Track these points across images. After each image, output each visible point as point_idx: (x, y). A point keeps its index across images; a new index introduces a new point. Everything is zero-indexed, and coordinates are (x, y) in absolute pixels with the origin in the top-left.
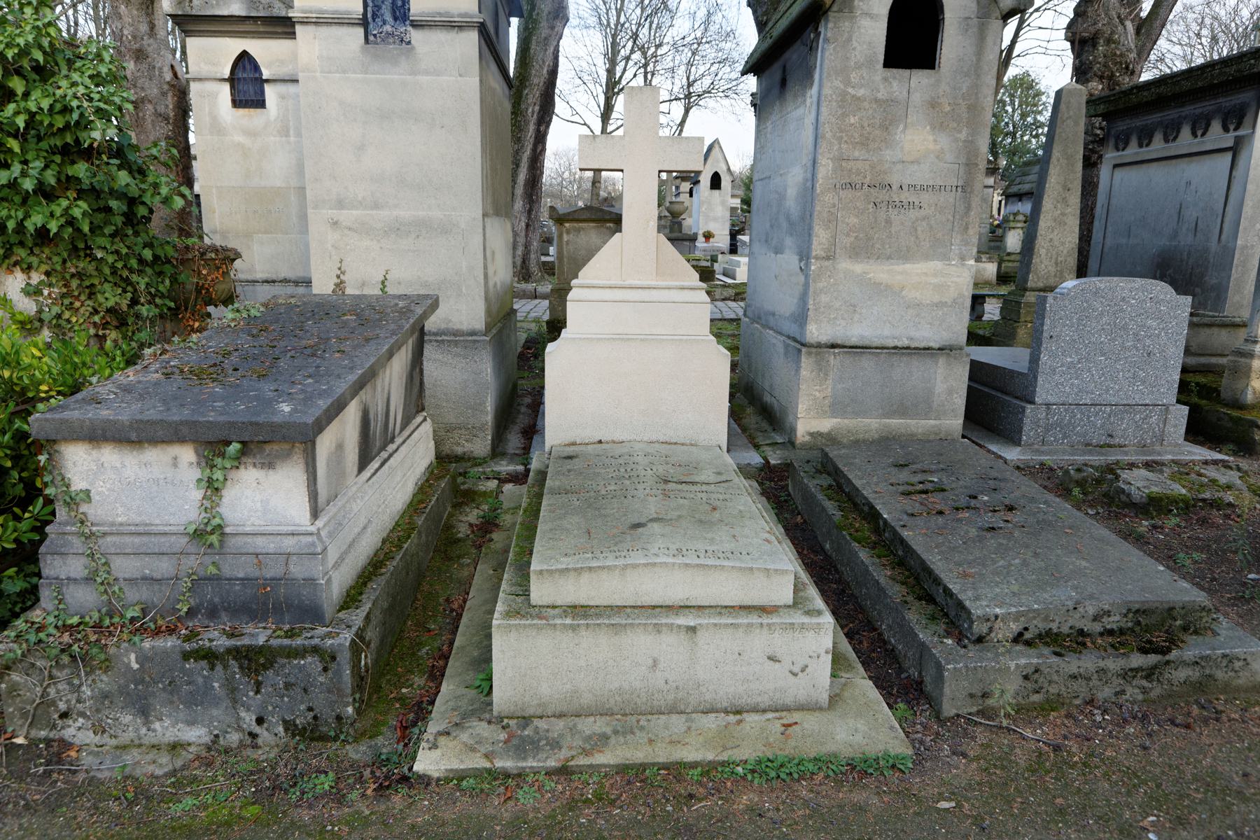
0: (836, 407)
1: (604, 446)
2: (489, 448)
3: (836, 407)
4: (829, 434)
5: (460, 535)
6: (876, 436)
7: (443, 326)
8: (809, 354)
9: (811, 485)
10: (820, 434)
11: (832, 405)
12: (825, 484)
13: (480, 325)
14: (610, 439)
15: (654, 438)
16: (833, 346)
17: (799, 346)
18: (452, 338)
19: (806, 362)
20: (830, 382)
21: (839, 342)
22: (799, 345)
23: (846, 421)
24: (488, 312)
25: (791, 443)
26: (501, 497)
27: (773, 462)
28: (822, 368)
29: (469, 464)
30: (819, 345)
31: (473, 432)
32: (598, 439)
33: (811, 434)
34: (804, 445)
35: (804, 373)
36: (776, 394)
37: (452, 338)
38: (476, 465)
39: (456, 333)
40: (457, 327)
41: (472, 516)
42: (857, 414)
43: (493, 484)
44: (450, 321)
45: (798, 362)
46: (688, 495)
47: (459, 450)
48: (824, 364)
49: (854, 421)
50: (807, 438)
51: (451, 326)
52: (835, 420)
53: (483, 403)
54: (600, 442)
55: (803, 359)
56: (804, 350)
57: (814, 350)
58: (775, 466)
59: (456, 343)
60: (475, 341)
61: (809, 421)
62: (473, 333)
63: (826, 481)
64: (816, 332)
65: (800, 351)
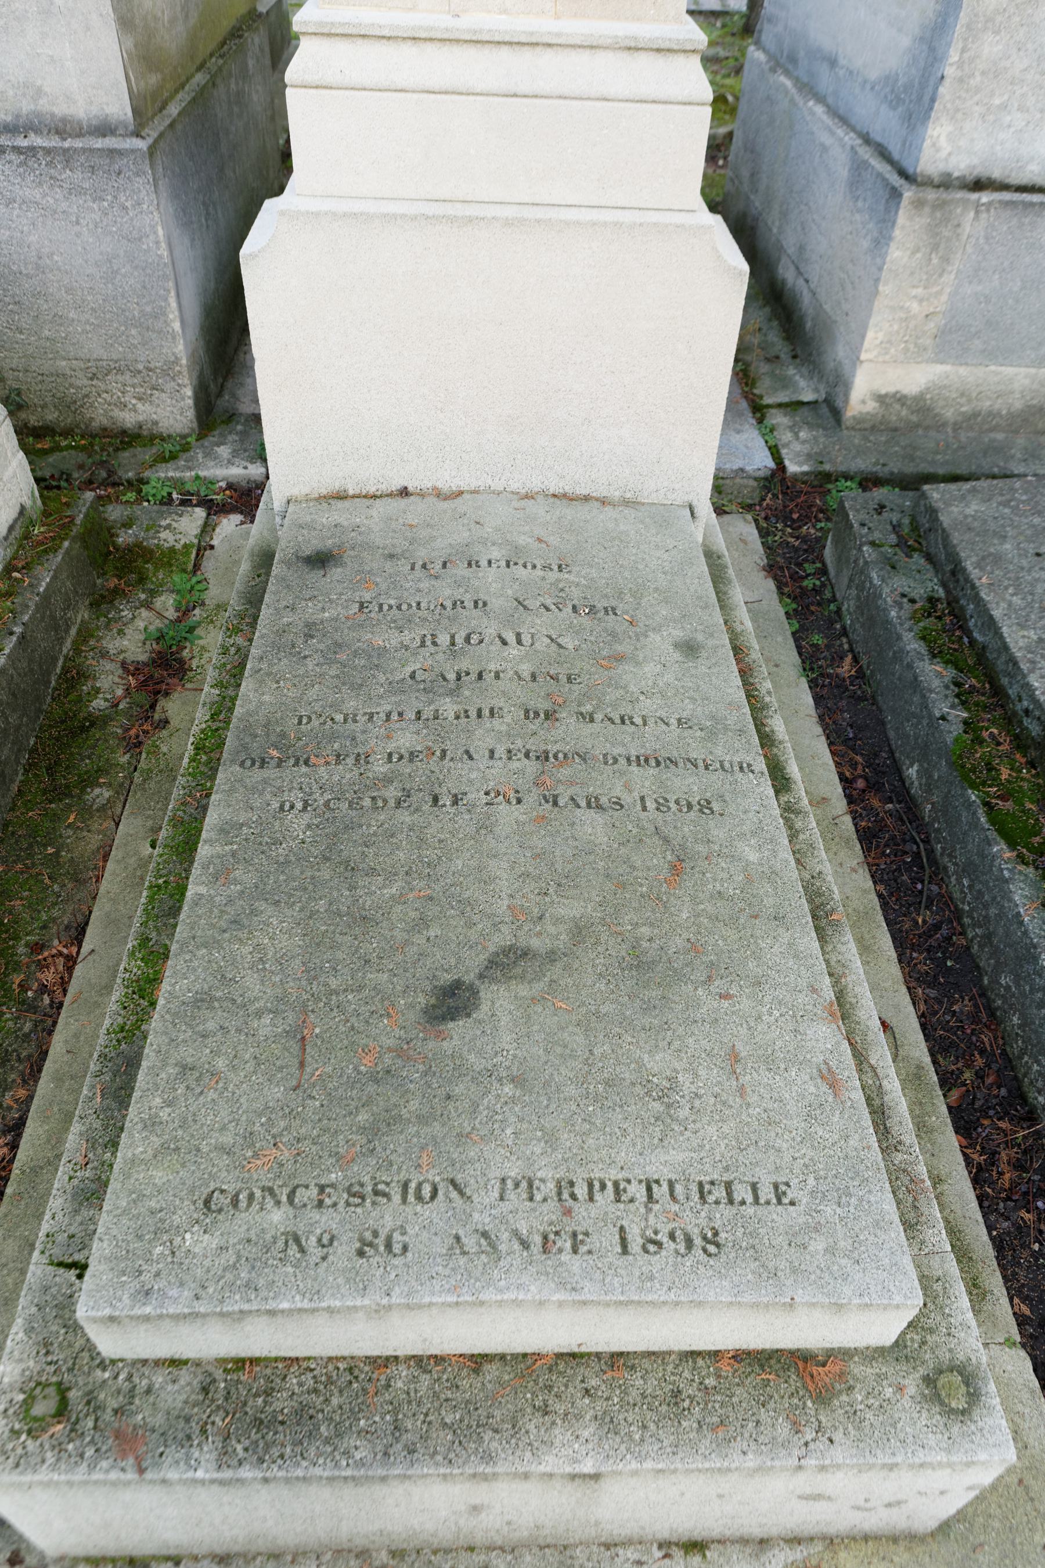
0: (951, 339)
1: (414, 511)
2: (191, 414)
3: (951, 339)
4: (919, 398)
5: (99, 704)
6: (1018, 405)
7: (26, 107)
8: (919, 204)
9: (888, 595)
10: (900, 399)
11: (943, 335)
12: (919, 592)
13: (118, 106)
14: (427, 485)
15: (535, 483)
16: (979, 185)
17: (895, 180)
18: (54, 142)
19: (908, 225)
20: (949, 278)
21: (996, 174)
22: (895, 176)
23: (963, 371)
24: (143, 57)
25: (828, 410)
26: (209, 565)
27: (793, 468)
28: (938, 244)
29: (147, 455)
30: (946, 183)
31: (151, 379)
32: (396, 485)
33: (881, 399)
34: (859, 420)
35: (897, 254)
36: (814, 280)
37: (54, 142)
38: (163, 459)
39: (63, 128)
40: (61, 109)
41: (132, 637)
42: (991, 355)
43: (190, 523)
44: (39, 92)
45: (886, 221)
46: (609, 785)
47: (128, 419)
48: (946, 233)
49: (980, 371)
50: (871, 406)
51: (43, 105)
52: (940, 369)
53: (160, 313)
54: (404, 492)
55: (902, 218)
56: (909, 194)
57: (931, 195)
58: (795, 477)
59: (68, 156)
60: (112, 153)
61: (885, 364)
62: (104, 129)
63: (919, 582)
64: (947, 145)
65: (895, 194)
